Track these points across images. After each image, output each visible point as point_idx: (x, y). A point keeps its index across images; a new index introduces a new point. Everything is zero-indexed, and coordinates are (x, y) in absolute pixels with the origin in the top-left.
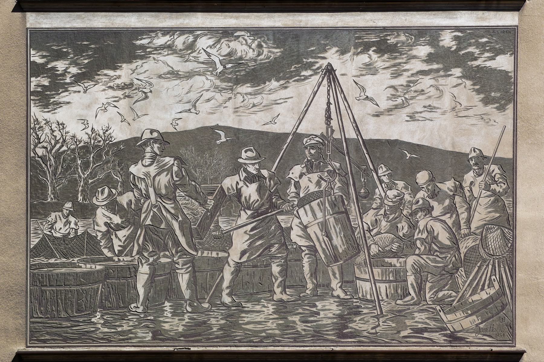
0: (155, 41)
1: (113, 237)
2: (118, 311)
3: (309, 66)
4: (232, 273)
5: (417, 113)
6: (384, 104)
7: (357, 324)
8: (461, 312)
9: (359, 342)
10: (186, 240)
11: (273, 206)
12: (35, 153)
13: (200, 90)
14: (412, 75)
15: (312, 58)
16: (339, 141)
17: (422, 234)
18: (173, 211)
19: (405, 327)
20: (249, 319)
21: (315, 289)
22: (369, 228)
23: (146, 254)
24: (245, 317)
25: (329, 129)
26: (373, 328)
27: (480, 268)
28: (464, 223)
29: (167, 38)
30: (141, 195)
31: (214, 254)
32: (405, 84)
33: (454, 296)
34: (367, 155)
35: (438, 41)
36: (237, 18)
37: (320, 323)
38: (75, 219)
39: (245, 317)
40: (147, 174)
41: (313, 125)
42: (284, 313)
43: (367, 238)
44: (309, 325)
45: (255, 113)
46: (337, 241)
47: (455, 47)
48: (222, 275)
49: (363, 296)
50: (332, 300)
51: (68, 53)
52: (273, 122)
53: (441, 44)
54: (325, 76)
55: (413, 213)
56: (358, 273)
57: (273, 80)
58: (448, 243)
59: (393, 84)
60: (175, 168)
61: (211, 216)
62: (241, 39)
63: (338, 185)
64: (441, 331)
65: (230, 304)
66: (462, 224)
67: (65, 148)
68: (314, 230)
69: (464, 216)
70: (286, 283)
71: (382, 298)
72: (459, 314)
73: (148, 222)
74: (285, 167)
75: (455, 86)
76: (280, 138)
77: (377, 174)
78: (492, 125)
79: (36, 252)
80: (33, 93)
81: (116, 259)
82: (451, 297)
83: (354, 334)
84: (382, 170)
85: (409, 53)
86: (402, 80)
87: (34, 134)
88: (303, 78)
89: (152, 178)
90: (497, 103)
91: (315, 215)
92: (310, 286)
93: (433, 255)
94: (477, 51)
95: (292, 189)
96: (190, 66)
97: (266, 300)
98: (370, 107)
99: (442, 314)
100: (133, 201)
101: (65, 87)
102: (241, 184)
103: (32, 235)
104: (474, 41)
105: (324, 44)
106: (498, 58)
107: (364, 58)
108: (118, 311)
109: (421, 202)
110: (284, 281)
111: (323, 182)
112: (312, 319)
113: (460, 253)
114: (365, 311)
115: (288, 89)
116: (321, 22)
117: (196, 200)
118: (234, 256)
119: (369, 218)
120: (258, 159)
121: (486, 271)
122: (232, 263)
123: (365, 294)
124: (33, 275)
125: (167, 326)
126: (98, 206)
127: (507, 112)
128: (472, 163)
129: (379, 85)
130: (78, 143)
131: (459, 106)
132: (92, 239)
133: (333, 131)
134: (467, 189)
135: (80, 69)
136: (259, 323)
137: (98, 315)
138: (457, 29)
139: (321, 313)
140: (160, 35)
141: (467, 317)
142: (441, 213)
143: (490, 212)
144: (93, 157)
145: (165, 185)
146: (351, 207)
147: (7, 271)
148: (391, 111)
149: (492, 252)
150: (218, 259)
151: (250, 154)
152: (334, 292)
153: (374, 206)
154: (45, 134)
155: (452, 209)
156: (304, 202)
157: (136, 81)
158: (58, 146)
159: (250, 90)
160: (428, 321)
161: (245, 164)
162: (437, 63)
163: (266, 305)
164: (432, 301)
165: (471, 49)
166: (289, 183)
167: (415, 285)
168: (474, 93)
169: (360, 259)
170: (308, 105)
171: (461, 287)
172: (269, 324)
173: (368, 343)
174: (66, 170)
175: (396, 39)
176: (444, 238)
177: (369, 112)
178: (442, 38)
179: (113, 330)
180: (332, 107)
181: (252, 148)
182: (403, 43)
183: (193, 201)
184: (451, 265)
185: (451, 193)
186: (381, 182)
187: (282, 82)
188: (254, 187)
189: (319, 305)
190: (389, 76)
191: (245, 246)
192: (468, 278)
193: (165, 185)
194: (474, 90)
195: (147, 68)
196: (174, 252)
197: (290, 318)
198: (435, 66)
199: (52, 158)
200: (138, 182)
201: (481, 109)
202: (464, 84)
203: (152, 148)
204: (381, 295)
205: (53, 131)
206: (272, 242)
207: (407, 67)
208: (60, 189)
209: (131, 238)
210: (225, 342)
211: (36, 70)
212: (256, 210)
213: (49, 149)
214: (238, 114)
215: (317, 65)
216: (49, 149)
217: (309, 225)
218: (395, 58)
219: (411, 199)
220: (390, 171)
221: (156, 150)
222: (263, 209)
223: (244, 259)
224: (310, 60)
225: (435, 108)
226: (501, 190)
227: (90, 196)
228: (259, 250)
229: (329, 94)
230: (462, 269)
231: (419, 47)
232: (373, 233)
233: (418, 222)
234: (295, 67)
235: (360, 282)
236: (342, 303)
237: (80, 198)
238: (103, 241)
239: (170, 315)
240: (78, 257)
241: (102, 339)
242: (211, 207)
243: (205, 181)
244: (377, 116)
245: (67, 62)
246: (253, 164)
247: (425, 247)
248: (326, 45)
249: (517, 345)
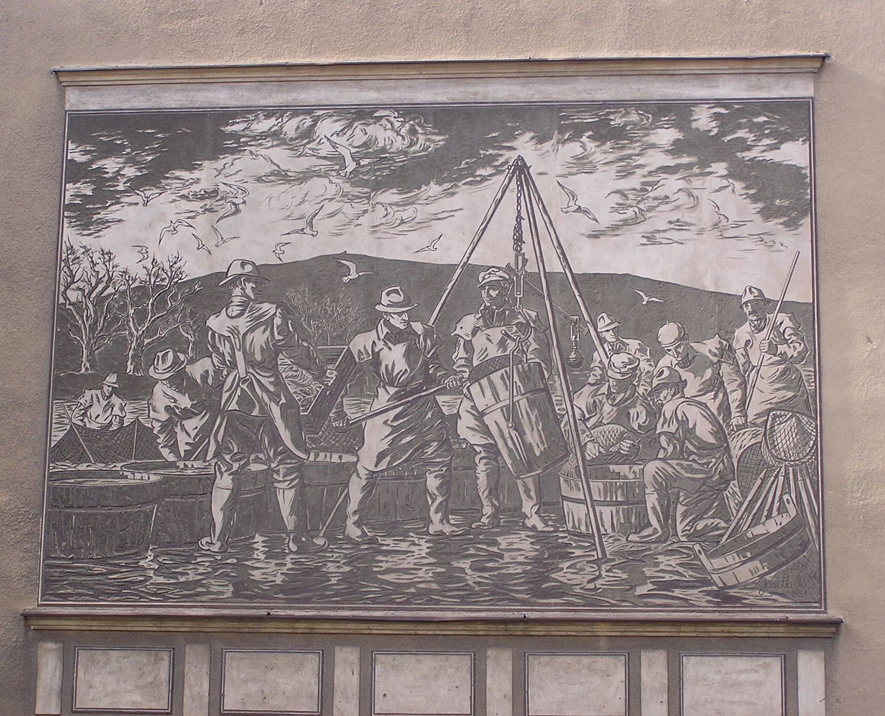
0: (253, 127)
1: (178, 429)
2: (181, 549)
3: (488, 161)
4: (363, 489)
5: (659, 231)
6: (606, 219)
7: (564, 574)
8: (735, 555)
9: (568, 604)
10: (291, 435)
11: (430, 381)
12: (66, 298)
13: (319, 200)
14: (650, 173)
15: (494, 148)
16: (534, 278)
17: (669, 426)
18: (272, 389)
19: (644, 580)
20: (388, 565)
21: (494, 516)
22: (584, 416)
23: (227, 458)
24: (382, 561)
25: (520, 258)
26: (590, 581)
27: (763, 481)
28: (738, 407)
29: (273, 121)
30: (223, 362)
31: (335, 458)
32: (638, 187)
33: (724, 528)
34: (579, 299)
35: (691, 121)
36: (378, 90)
37: (504, 571)
38: (120, 401)
39: (382, 561)
40: (234, 331)
41: (496, 252)
42: (447, 554)
43: (580, 432)
44: (486, 575)
45: (403, 233)
46: (532, 437)
47: (716, 131)
48: (346, 491)
49: (574, 526)
50: (523, 534)
51: (124, 147)
52: (431, 247)
53: (694, 125)
54: (513, 177)
56: (565, 491)
57: (432, 183)
58: (711, 440)
59: (620, 188)
60: (278, 321)
61: (329, 398)
63: (534, 346)
64: (702, 587)
65: (360, 540)
66: (733, 409)
67: (110, 290)
68: (495, 419)
69: (735, 397)
70: (450, 505)
71: (606, 530)
72: (732, 559)
73: (233, 406)
74: (450, 317)
75: (717, 191)
76: (441, 272)
77: (596, 330)
78: (778, 251)
79: (60, 452)
80: (69, 207)
81: (181, 465)
82: (718, 529)
83: (561, 591)
84: (604, 323)
85: (643, 139)
86: (634, 182)
87: (66, 269)
88: (478, 179)
89: (241, 337)
90: (785, 216)
91: (497, 394)
92: (488, 510)
93: (687, 460)
94: (751, 137)
95: (461, 352)
96: (304, 163)
97: (417, 534)
98: (584, 224)
99: (703, 557)
100: (211, 373)
101: (115, 197)
102: (380, 345)
103: (54, 426)
104: (745, 120)
105: (512, 127)
106: (784, 146)
107: (574, 149)
108: (181, 549)
109: (666, 373)
110: (446, 501)
111: (509, 341)
112: (491, 565)
113: (731, 457)
114: (578, 552)
115: (456, 196)
116: (507, 94)
117: (308, 369)
118: (367, 460)
119: (582, 400)
120: (407, 305)
121: (774, 486)
122: (363, 473)
123: (577, 525)
124: (53, 490)
125: (257, 575)
126: (156, 382)
127: (800, 230)
128: (747, 310)
129: (599, 189)
130: (131, 282)
131: (724, 221)
132: (145, 433)
133: (525, 261)
134: (739, 354)
135: (140, 170)
136: (405, 571)
137: (150, 555)
138: (719, 102)
139: (506, 555)
140: (261, 117)
141: (744, 563)
142: (700, 391)
143: (778, 390)
144: (153, 304)
145: (261, 346)
146: (555, 382)
147: (13, 483)
148: (618, 229)
149: (783, 454)
150: (341, 466)
151: (395, 298)
152: (526, 521)
153: (592, 380)
155: (716, 385)
156: (480, 373)
157: (222, 188)
158: (100, 287)
159: (397, 198)
160: (680, 569)
161: (386, 313)
162: (689, 156)
163: (417, 542)
164: (688, 536)
165: (740, 134)
166: (456, 343)
167: (659, 510)
168: (748, 200)
169: (569, 466)
170: (487, 221)
171: (734, 512)
172: (421, 573)
173: (583, 606)
174: (111, 324)
175: (624, 119)
176: (704, 430)
177: (583, 231)
178: (696, 118)
179: (172, 581)
180: (525, 224)
181: (398, 288)
182: (635, 124)
183: (304, 372)
184: (717, 476)
185: (715, 359)
186: (602, 341)
187: (446, 186)
188: (399, 350)
189: (503, 541)
190: (613, 175)
191: (385, 446)
192: (745, 497)
193: (261, 346)
194: (748, 196)
195: (241, 167)
196: (271, 454)
197: (455, 564)
198: (685, 160)
199: (90, 306)
200: (220, 342)
201: (759, 225)
202: (731, 187)
203: (242, 289)
204: (603, 526)
205: (95, 265)
206: (428, 438)
207: (641, 161)
208: (100, 353)
209: (205, 432)
210: (349, 601)
211: (75, 172)
212: (403, 386)
213: (87, 291)
214: (377, 235)
215: (501, 160)
216: (87, 291)
217: (487, 411)
218: (623, 148)
219: (651, 369)
220: (616, 324)
221: (249, 291)
222: (414, 384)
223: (383, 465)
224: (490, 152)
225: (686, 224)
226: (795, 355)
227: (146, 365)
228: (407, 451)
229: (519, 204)
230: (736, 482)
231: (659, 130)
232: (589, 424)
233: (662, 405)
234: (467, 163)
235: (570, 504)
236: (539, 537)
237: (130, 367)
238: (162, 436)
239: (262, 557)
240: (122, 461)
241: (155, 594)
242: (332, 381)
243: (323, 339)
244: (596, 237)
245: (121, 160)
246: (400, 314)
247: (675, 447)
248: (515, 129)
249: (828, 611)
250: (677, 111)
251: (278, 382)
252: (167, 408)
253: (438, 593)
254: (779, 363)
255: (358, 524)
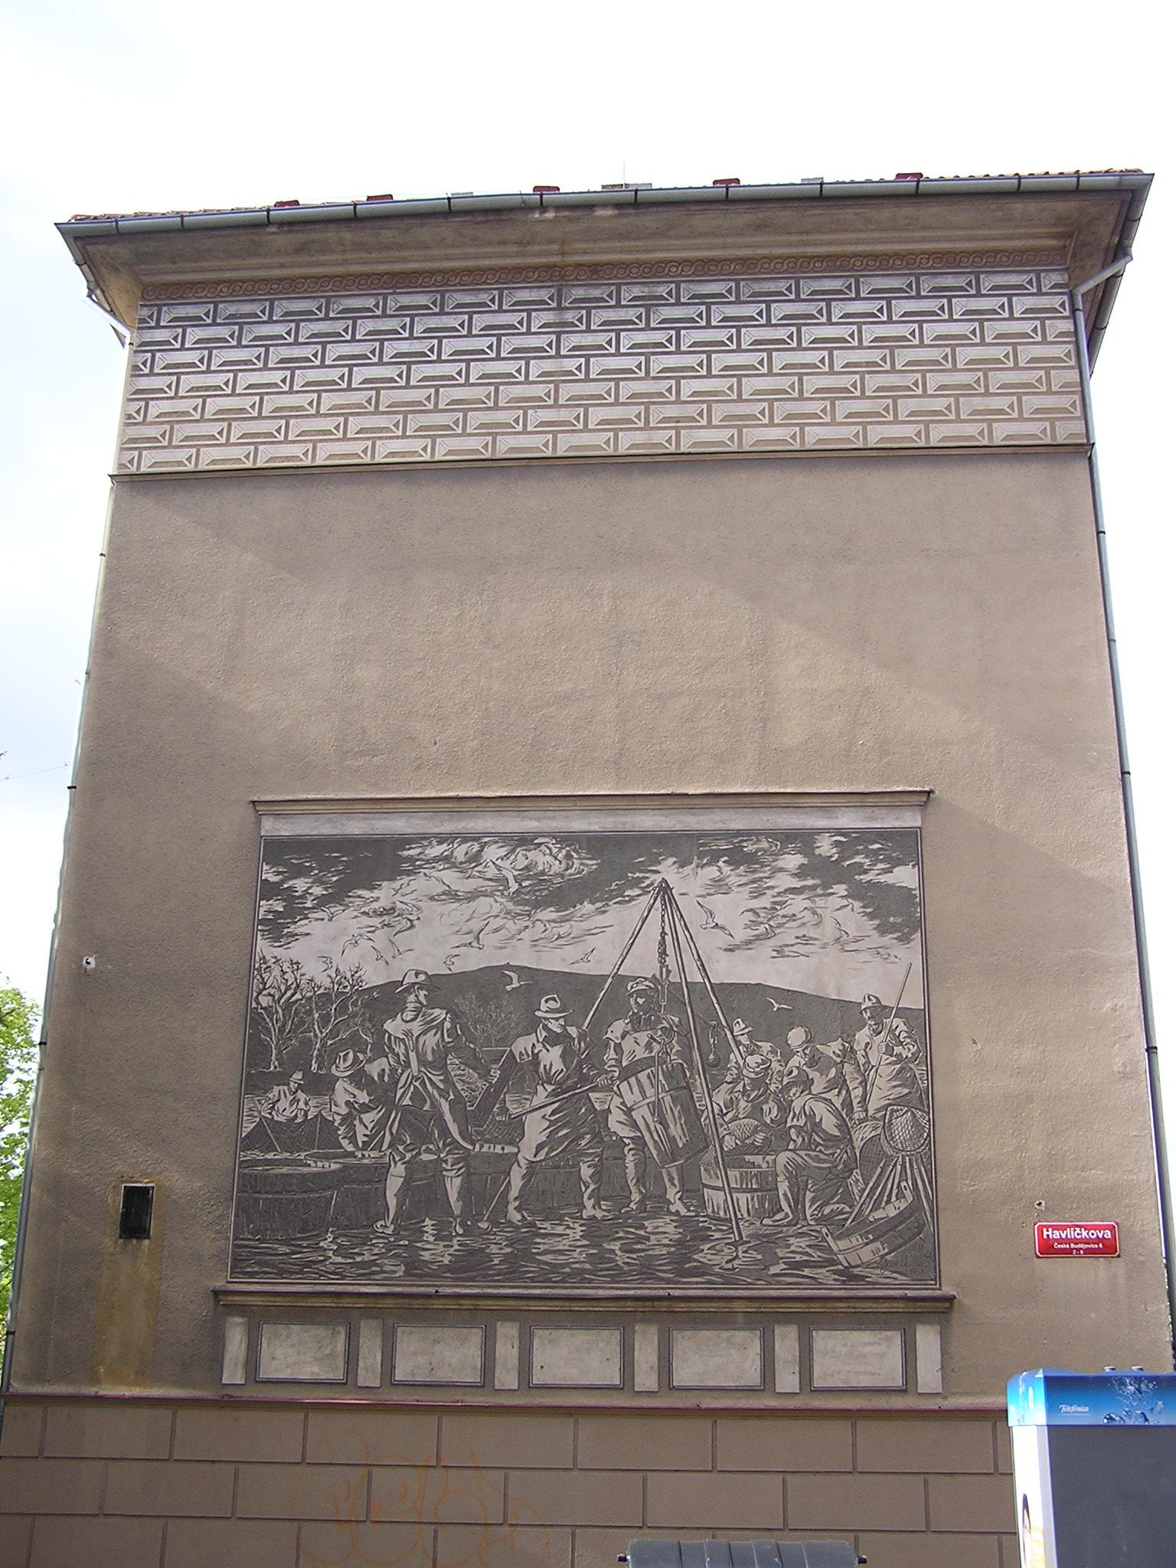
1: (356, 1122)
4: (523, 1177)
6: (741, 935)
7: (705, 1255)
11: (584, 1079)
12: (258, 1003)
18: (442, 1086)
21: (641, 1202)
23: (401, 1148)
29: (445, 846)
31: (498, 1149)
32: (769, 906)
36: (538, 819)
40: (408, 1033)
41: (643, 964)
46: (675, 1131)
50: (668, 1219)
51: (314, 869)
55: (787, 1088)
60: (447, 1025)
61: (493, 1095)
62: (543, 847)
63: (677, 1048)
67: (298, 996)
68: (641, 1114)
72: (856, 1240)
73: (407, 1101)
74: (602, 1022)
80: (261, 922)
83: (702, 1270)
86: (765, 902)
92: (636, 1197)
94: (867, 862)
95: (612, 1054)
96: (472, 884)
98: (722, 939)
99: (829, 1239)
101: (304, 914)
102: (539, 1047)
107: (712, 872)
112: (639, 1246)
114: (717, 1235)
117: (474, 1069)
118: (527, 1150)
119: (720, 1097)
122: (523, 1162)
124: (242, 1176)
125: (426, 1256)
127: (912, 944)
128: (866, 1016)
129: (733, 908)
133: (669, 972)
134: (860, 1055)
135: (326, 889)
136: (561, 1252)
137: (330, 1237)
138: (839, 831)
140: (434, 843)
151: (552, 1005)
154: (273, 977)
155: (839, 1083)
156: (628, 1072)
157: (399, 905)
158: (289, 993)
160: (810, 1251)
164: (816, 1220)
165: (857, 859)
166: (607, 1046)
172: (575, 1255)
174: (298, 1027)
176: (829, 1124)
180: (668, 938)
185: (839, 1060)
186: (738, 1044)
188: (557, 1050)
198: (810, 882)
201: (876, 940)
209: (381, 1125)
211: (269, 890)
212: (560, 1084)
218: (754, 872)
223: (541, 1156)
232: (726, 1119)
236: (682, 1221)
237: (314, 1066)
239: (432, 1239)
244: (731, 950)
250: (804, 840)
251: (448, 1081)
252: (347, 1103)
253: (590, 1272)
254: (895, 1063)
255: (518, 1209)
